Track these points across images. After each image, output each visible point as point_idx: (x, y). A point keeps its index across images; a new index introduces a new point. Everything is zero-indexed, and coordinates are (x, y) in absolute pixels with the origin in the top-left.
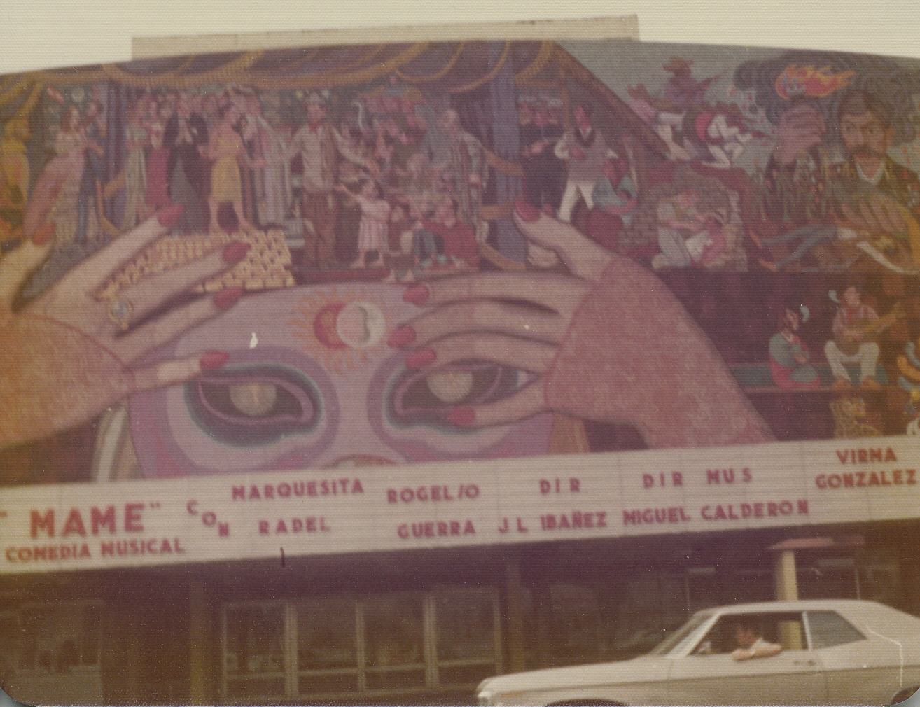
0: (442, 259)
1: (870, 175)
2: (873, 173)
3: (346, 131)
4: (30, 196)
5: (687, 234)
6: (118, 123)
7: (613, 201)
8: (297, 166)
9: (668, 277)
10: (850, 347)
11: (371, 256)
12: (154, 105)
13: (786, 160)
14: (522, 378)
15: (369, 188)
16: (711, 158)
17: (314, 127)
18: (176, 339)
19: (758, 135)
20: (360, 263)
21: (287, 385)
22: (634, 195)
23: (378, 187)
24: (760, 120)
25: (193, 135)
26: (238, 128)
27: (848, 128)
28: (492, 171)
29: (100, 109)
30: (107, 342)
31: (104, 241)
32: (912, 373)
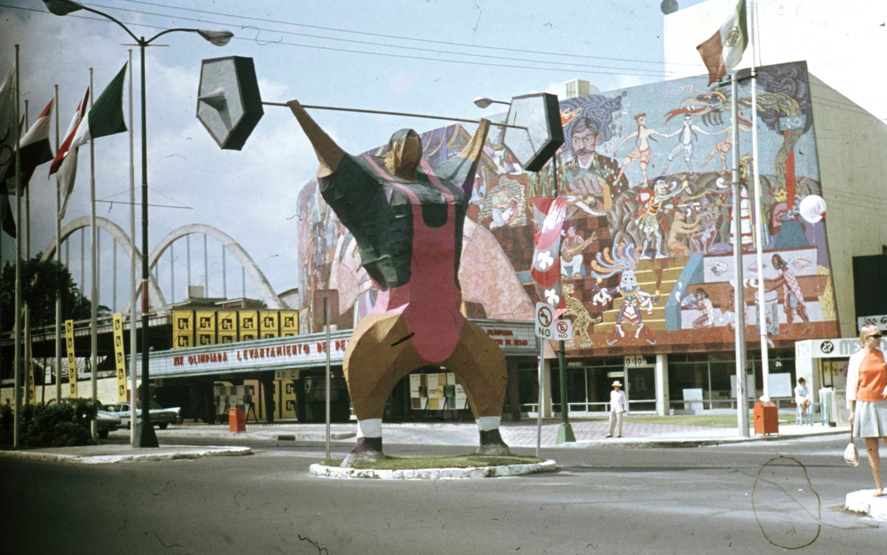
1: (584, 164)
2: (586, 163)
5: (503, 210)
9: (496, 232)
16: (514, 171)
22: (484, 195)
27: (576, 141)
32: (599, 269)
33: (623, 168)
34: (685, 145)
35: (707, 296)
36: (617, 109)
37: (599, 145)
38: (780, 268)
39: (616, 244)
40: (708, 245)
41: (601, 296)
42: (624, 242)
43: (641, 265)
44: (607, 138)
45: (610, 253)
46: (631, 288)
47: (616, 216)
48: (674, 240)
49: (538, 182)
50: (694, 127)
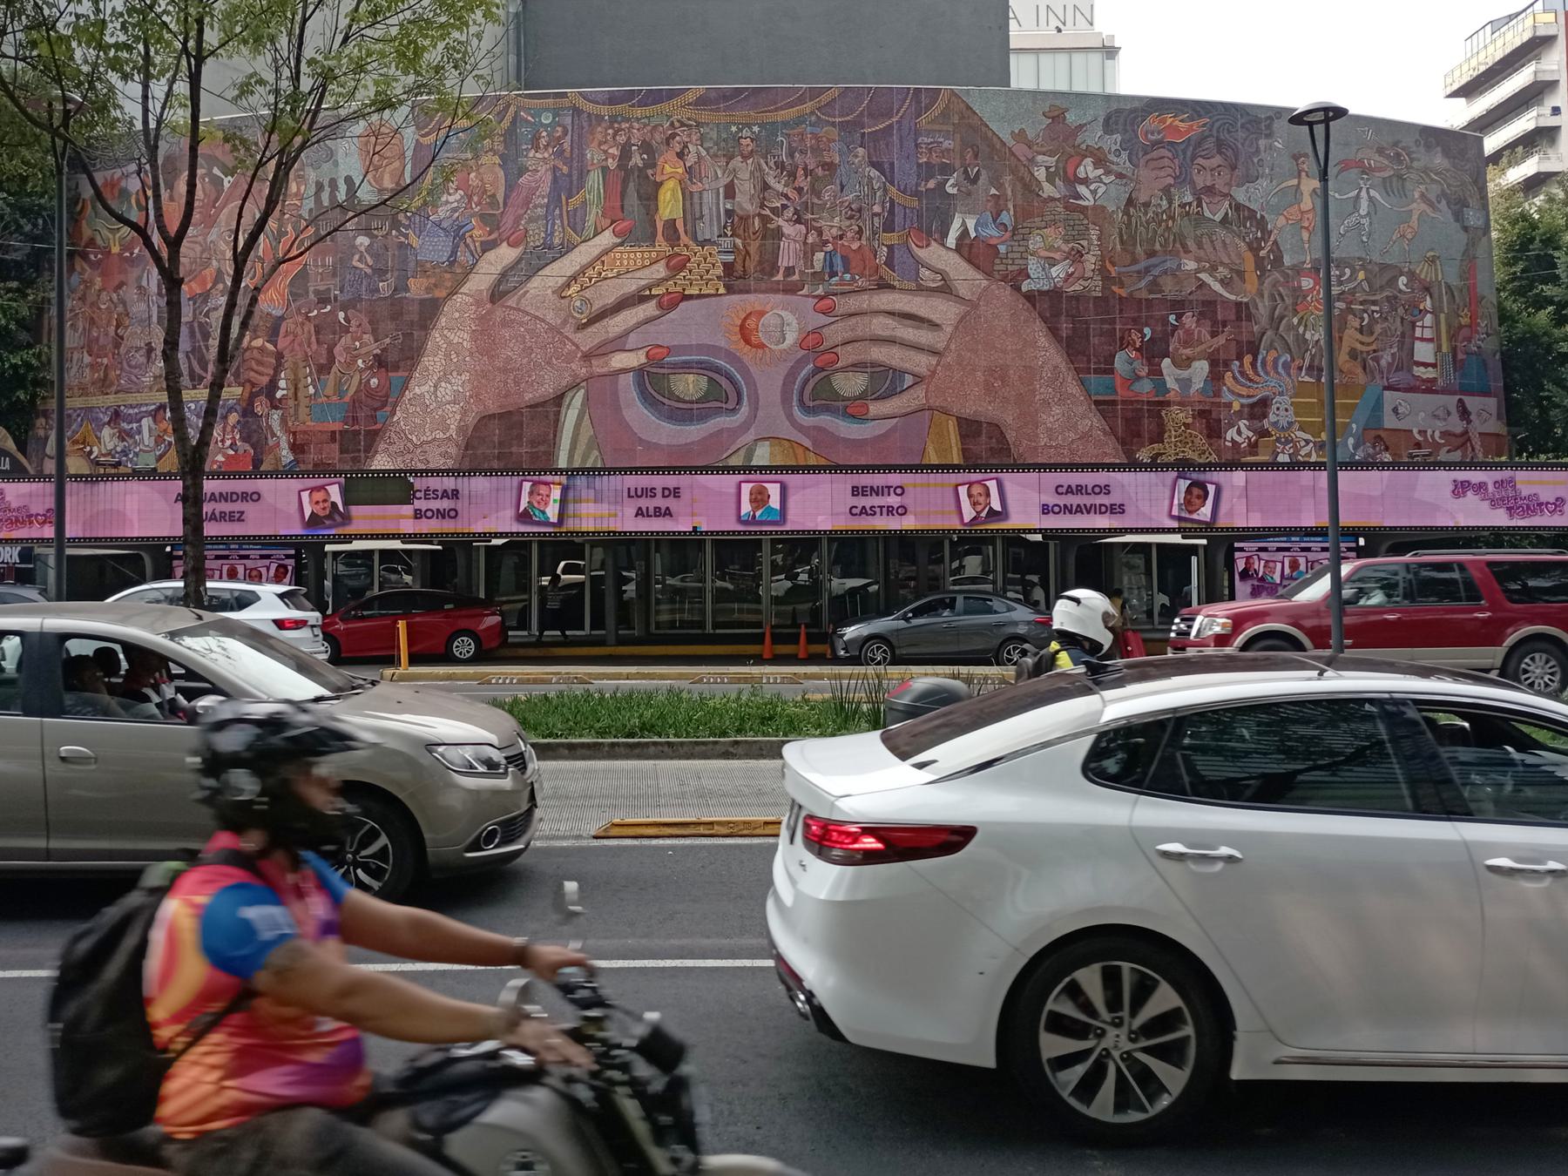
0: (848, 276)
2: (1216, 212)
3: (772, 164)
4: (505, 204)
5: (1053, 262)
6: (580, 145)
7: (992, 232)
8: (730, 192)
9: (1030, 297)
10: (1186, 363)
11: (789, 271)
12: (610, 131)
13: (1143, 198)
14: (909, 380)
15: (789, 213)
16: (1078, 196)
17: (745, 158)
18: (627, 333)
19: (1120, 176)
20: (780, 277)
21: (715, 376)
23: (796, 212)
24: (1122, 162)
25: (643, 159)
26: (681, 155)
27: (1199, 172)
28: (892, 201)
29: (565, 133)
30: (568, 331)
31: (566, 248)
33: (1275, 231)
34: (1362, 217)
35: (1387, 449)
36: (1268, 136)
37: (1238, 186)
38: (1465, 419)
39: (1263, 352)
40: (1389, 372)
41: (1239, 433)
42: (1276, 349)
43: (1300, 390)
44: (1250, 179)
45: (1254, 365)
46: (1286, 425)
47: (1265, 306)
48: (1347, 357)
49: (1129, 225)
50: (1372, 193)
